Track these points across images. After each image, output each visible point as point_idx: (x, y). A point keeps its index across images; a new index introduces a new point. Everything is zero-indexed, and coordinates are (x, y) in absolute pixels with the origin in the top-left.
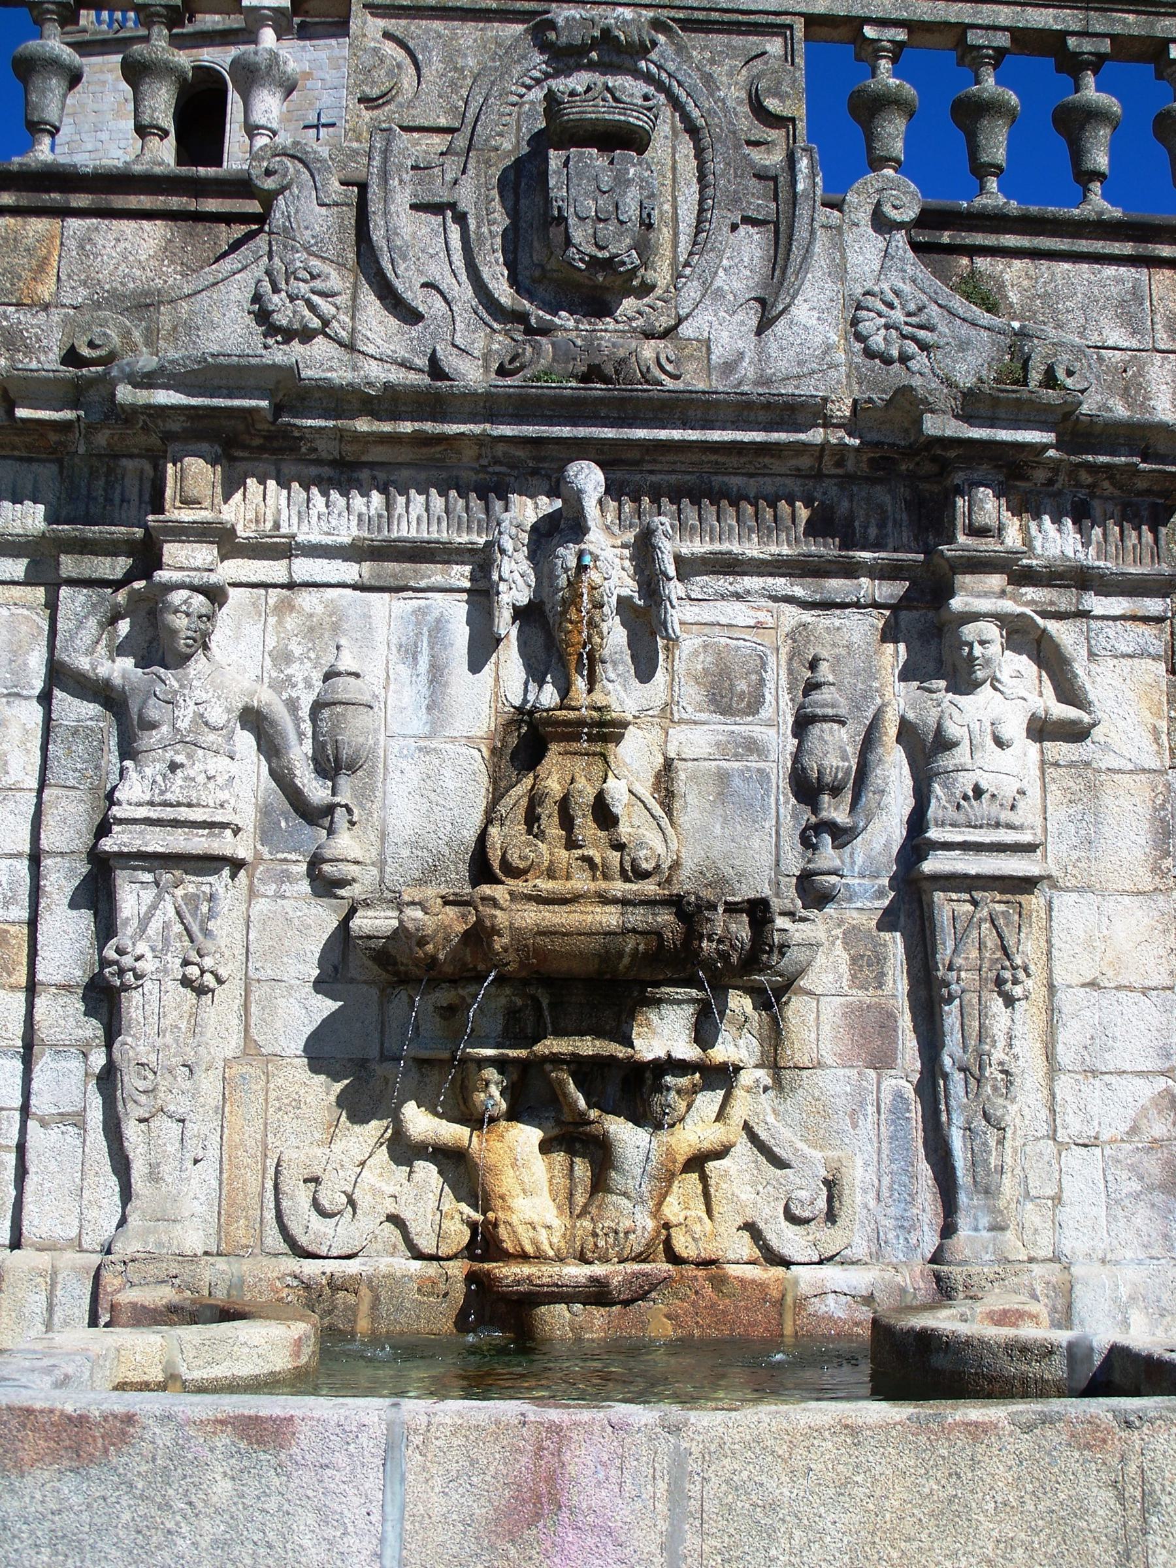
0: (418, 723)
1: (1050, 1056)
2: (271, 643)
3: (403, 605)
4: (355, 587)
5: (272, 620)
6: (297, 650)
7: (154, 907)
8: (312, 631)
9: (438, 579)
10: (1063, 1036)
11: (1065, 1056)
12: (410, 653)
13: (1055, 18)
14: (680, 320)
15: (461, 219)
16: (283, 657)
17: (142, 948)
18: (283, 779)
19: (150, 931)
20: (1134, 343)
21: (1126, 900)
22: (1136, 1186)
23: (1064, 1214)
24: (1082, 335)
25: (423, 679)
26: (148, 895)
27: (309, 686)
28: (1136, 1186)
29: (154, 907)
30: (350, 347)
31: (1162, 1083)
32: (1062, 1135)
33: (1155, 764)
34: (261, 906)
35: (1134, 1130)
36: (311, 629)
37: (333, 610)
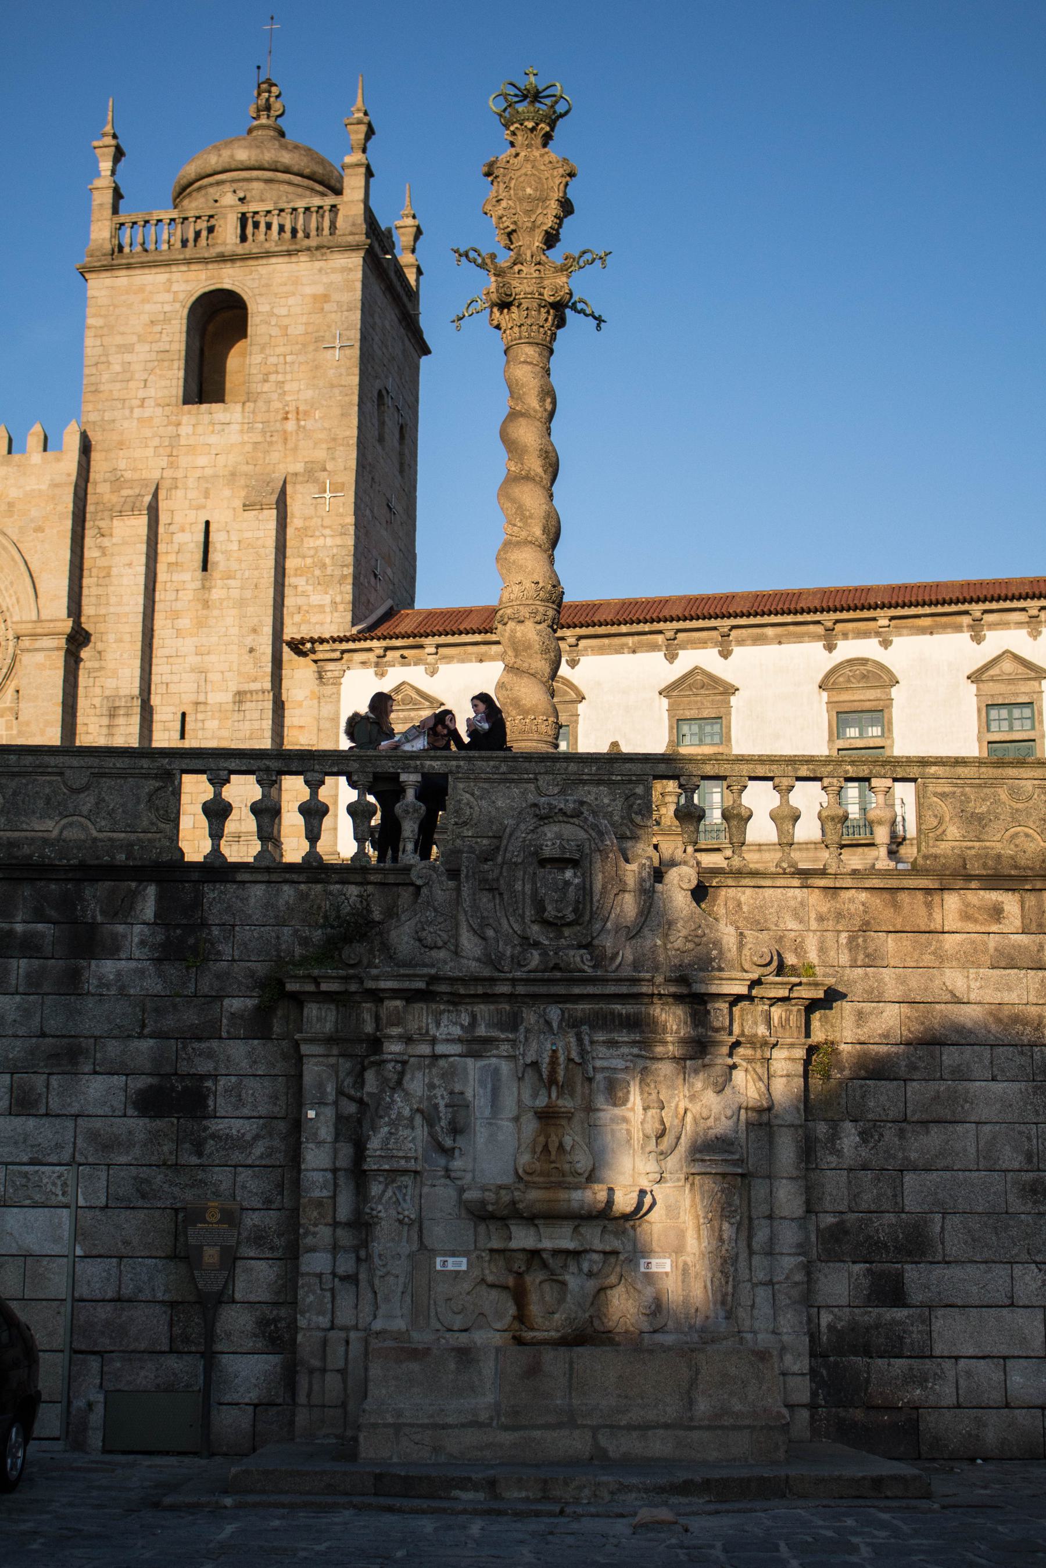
0: (487, 1112)
1: (749, 1245)
2: (427, 1081)
3: (481, 1063)
4: (459, 1056)
5: (427, 1071)
6: (436, 1081)
7: (384, 1191)
8: (443, 1076)
9: (495, 1052)
10: (755, 1240)
11: (756, 1246)
12: (482, 1083)
13: (770, 770)
14: (593, 938)
15: (501, 894)
16: (432, 1086)
17: (380, 1207)
18: (432, 1135)
19: (384, 1201)
20: (800, 927)
21: (784, 1181)
22: (788, 1301)
23: (756, 1312)
24: (776, 925)
25: (489, 1094)
26: (381, 1187)
27: (442, 1096)
28: (788, 1301)
29: (384, 1191)
30: (456, 953)
31: (801, 1258)
32: (755, 1280)
33: (797, 1122)
34: (426, 1190)
35: (787, 1278)
36: (443, 1074)
37: (452, 1065)
